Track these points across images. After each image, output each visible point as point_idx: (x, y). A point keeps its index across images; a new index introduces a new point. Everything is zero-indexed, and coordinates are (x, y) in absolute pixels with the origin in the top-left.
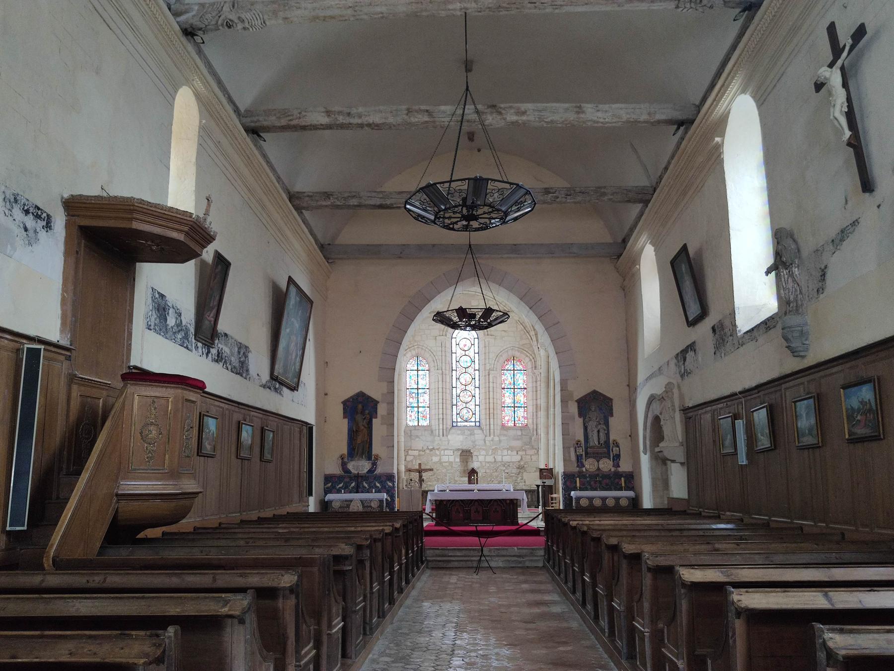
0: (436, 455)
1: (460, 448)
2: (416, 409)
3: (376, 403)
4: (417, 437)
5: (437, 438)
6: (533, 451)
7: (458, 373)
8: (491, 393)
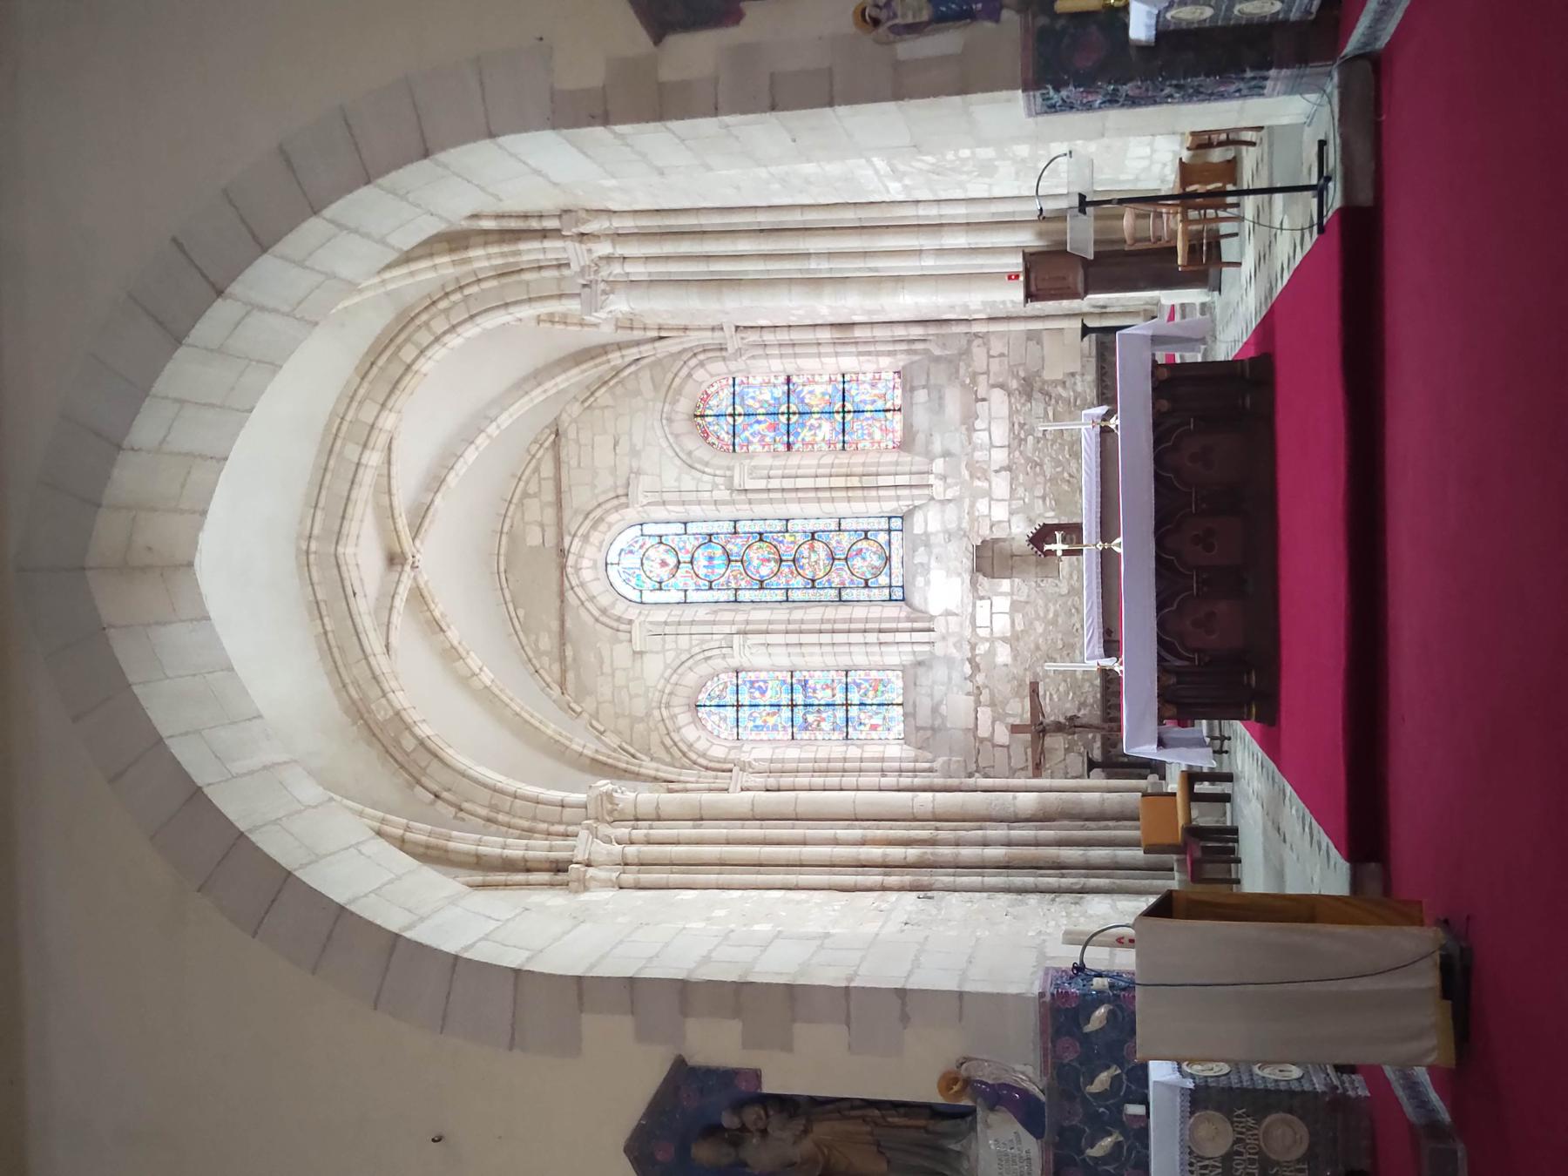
0: (991, 653)
1: (967, 577)
2: (854, 711)
3: (683, 1076)
4: (935, 710)
5: (939, 650)
7: (743, 584)
8: (801, 483)
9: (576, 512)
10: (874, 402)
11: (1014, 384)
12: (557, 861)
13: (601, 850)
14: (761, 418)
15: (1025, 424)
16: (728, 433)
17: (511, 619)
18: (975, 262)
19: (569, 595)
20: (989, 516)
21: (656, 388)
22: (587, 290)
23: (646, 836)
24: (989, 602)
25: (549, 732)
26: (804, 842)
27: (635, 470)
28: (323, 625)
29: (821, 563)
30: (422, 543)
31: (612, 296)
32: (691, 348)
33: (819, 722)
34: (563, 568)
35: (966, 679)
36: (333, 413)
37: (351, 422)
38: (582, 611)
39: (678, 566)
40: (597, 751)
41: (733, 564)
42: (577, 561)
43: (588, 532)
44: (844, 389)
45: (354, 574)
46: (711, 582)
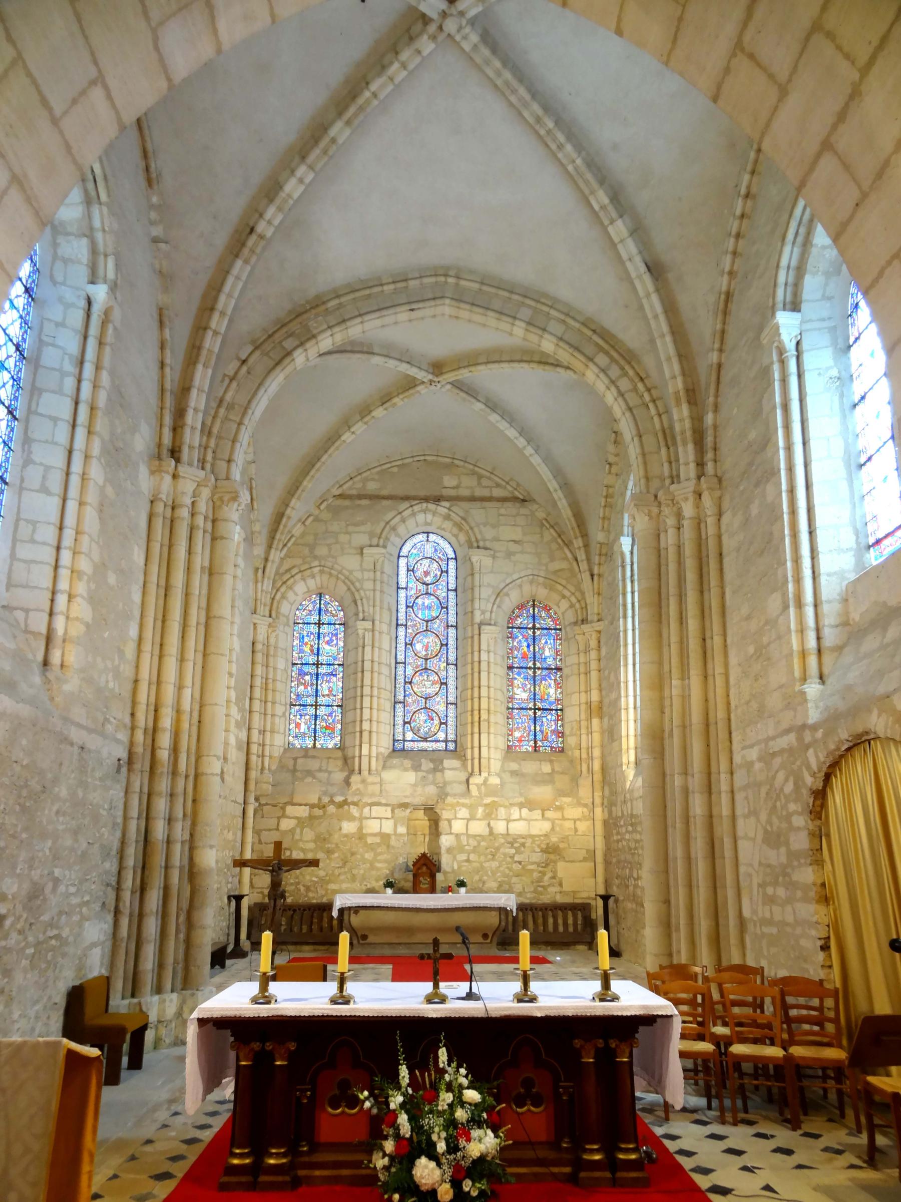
0: (352, 818)
4: (309, 773)
7: (410, 631)
9: (467, 512)
10: (542, 732)
11: (554, 839)
12: (180, 451)
13: (187, 486)
14: (532, 648)
15: (524, 847)
16: (521, 623)
17: (390, 462)
18: (678, 821)
19: (406, 504)
20: (456, 818)
21: (556, 572)
22: (653, 498)
23: (198, 527)
24: (390, 816)
25: (305, 483)
26: (182, 660)
27: (498, 554)
28: (389, 283)
30: (448, 390)
31: (647, 518)
32: (584, 598)
33: (304, 684)
34: (426, 499)
35: (332, 798)
36: (556, 300)
38: (396, 512)
40: (289, 518)
41: (425, 624)
42: (430, 511)
43: (452, 520)
44: (552, 710)
45: (428, 312)
46: (412, 607)
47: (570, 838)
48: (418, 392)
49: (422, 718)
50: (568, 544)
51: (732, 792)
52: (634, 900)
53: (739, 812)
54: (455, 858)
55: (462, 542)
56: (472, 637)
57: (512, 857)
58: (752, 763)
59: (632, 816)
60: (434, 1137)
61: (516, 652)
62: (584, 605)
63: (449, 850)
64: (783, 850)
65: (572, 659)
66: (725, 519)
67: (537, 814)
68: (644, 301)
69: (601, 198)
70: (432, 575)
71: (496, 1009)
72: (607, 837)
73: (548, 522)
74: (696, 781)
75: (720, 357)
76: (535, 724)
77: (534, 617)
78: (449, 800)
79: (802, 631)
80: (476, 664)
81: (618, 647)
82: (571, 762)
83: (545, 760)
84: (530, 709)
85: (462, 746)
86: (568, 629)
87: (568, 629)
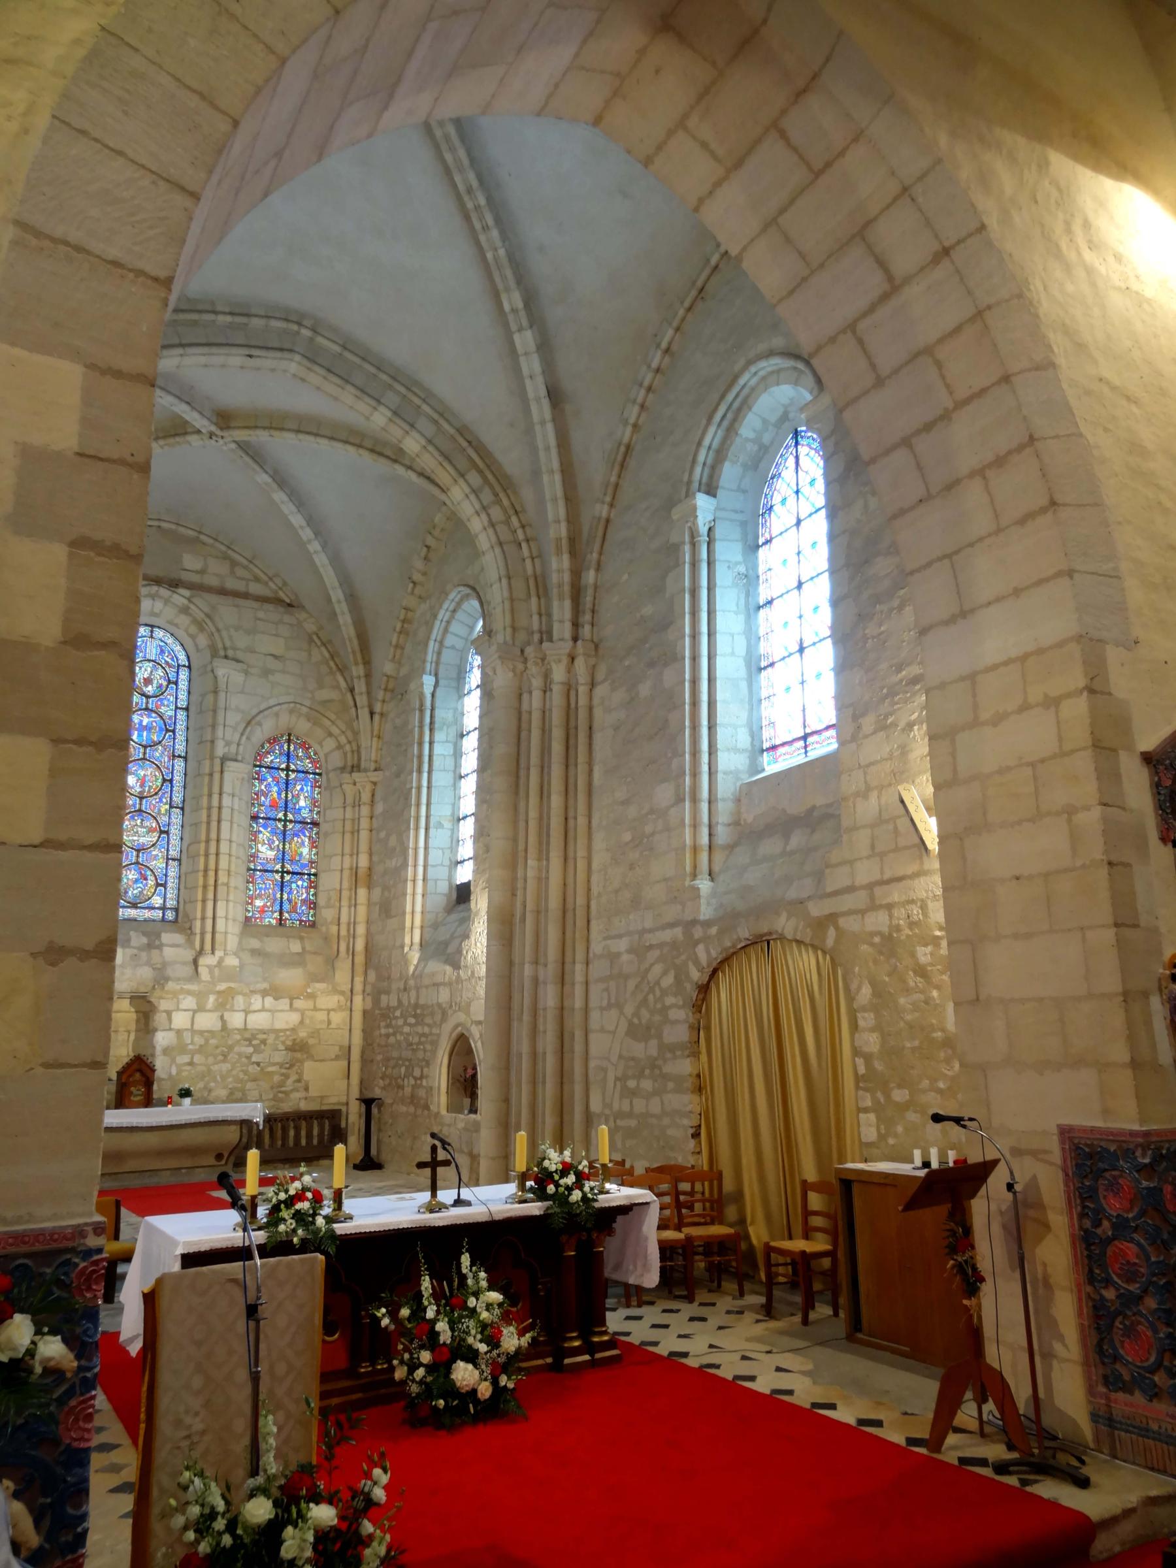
6: (336, 998)
10: (290, 901)
11: (302, 1034)
15: (265, 1045)
16: (272, 761)
20: (178, 1009)
21: (325, 702)
22: (519, 653)
28: (224, 313)
29: (135, 838)
30: (232, 450)
31: (511, 674)
37: (419, 407)
39: (143, 695)
41: (142, 750)
43: (190, 615)
44: (304, 874)
45: (268, 363)
47: (321, 1031)
48: (189, 443)
49: (130, 877)
50: (342, 669)
51: (587, 983)
52: (412, 1102)
53: (593, 1004)
54: (173, 1060)
55: (200, 647)
56: (211, 775)
57: (249, 1058)
58: (618, 955)
59: (416, 1006)
60: (470, 1340)
61: (263, 798)
62: (355, 748)
63: (166, 1051)
64: (653, 1043)
65: (337, 813)
66: (599, 691)
67: (284, 1004)
68: (538, 428)
69: (513, 300)
70: (155, 685)
71: (499, 1212)
72: (367, 1032)
73: (319, 638)
74: (549, 971)
75: (609, 512)
76: (282, 891)
77: (288, 755)
78: (171, 985)
79: (695, 826)
80: (215, 812)
81: (408, 805)
82: (326, 939)
83: (293, 937)
84: (277, 872)
85: (186, 915)
86: (331, 775)
87: (331, 775)
